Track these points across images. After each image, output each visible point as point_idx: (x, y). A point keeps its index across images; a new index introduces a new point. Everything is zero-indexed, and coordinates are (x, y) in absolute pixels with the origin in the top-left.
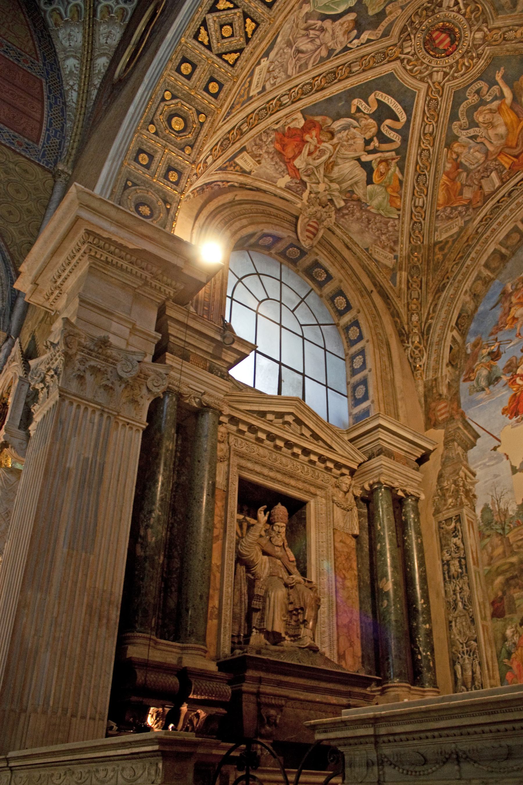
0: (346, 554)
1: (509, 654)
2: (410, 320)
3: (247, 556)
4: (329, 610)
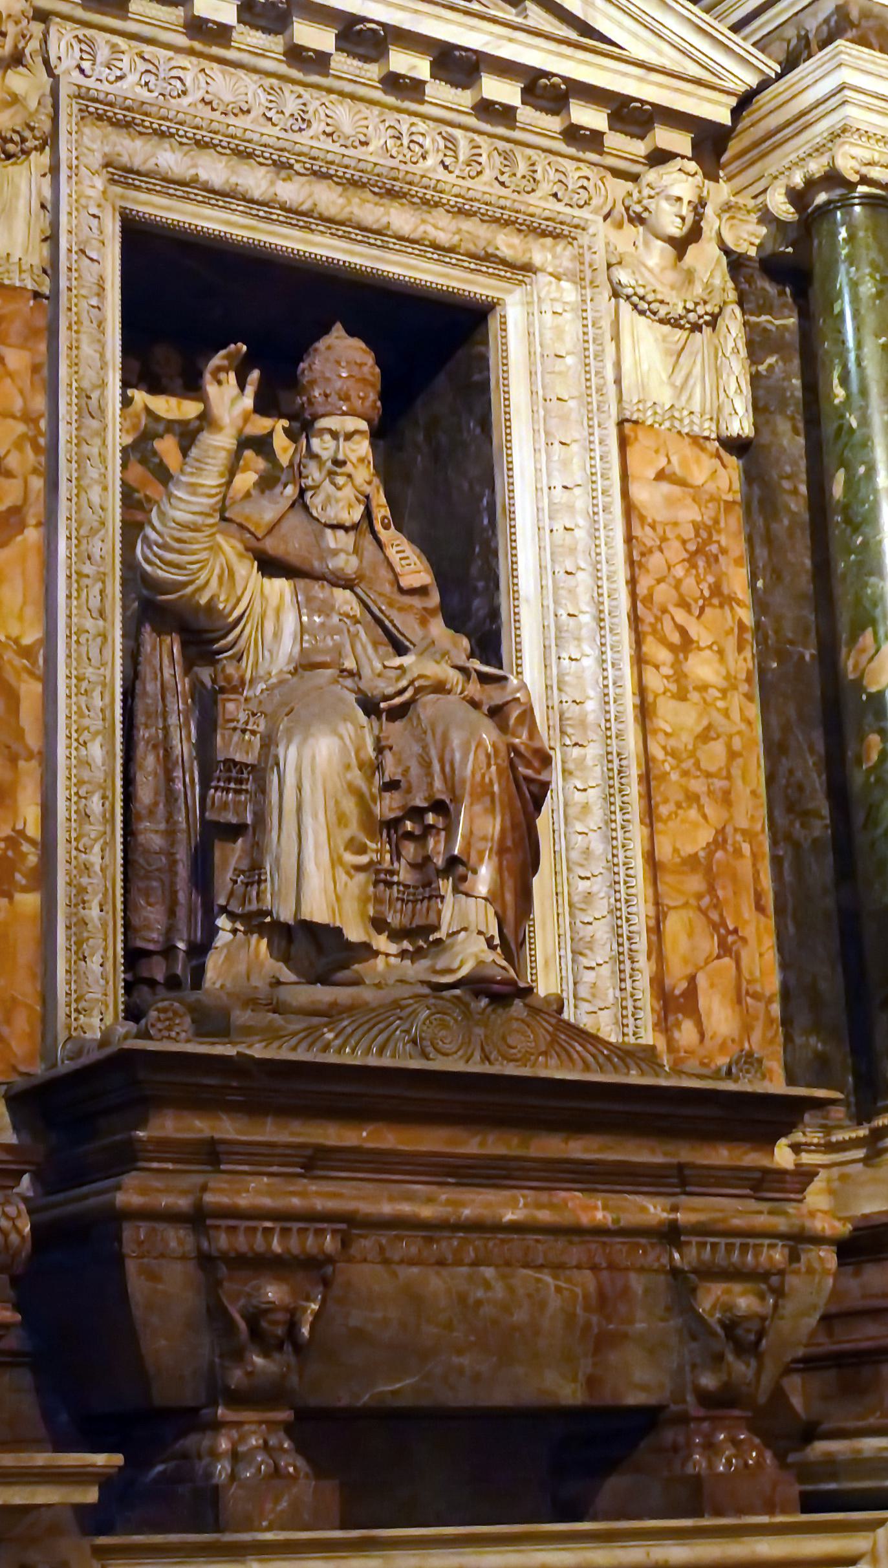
0: (689, 532)
3: (185, 585)
4: (608, 799)
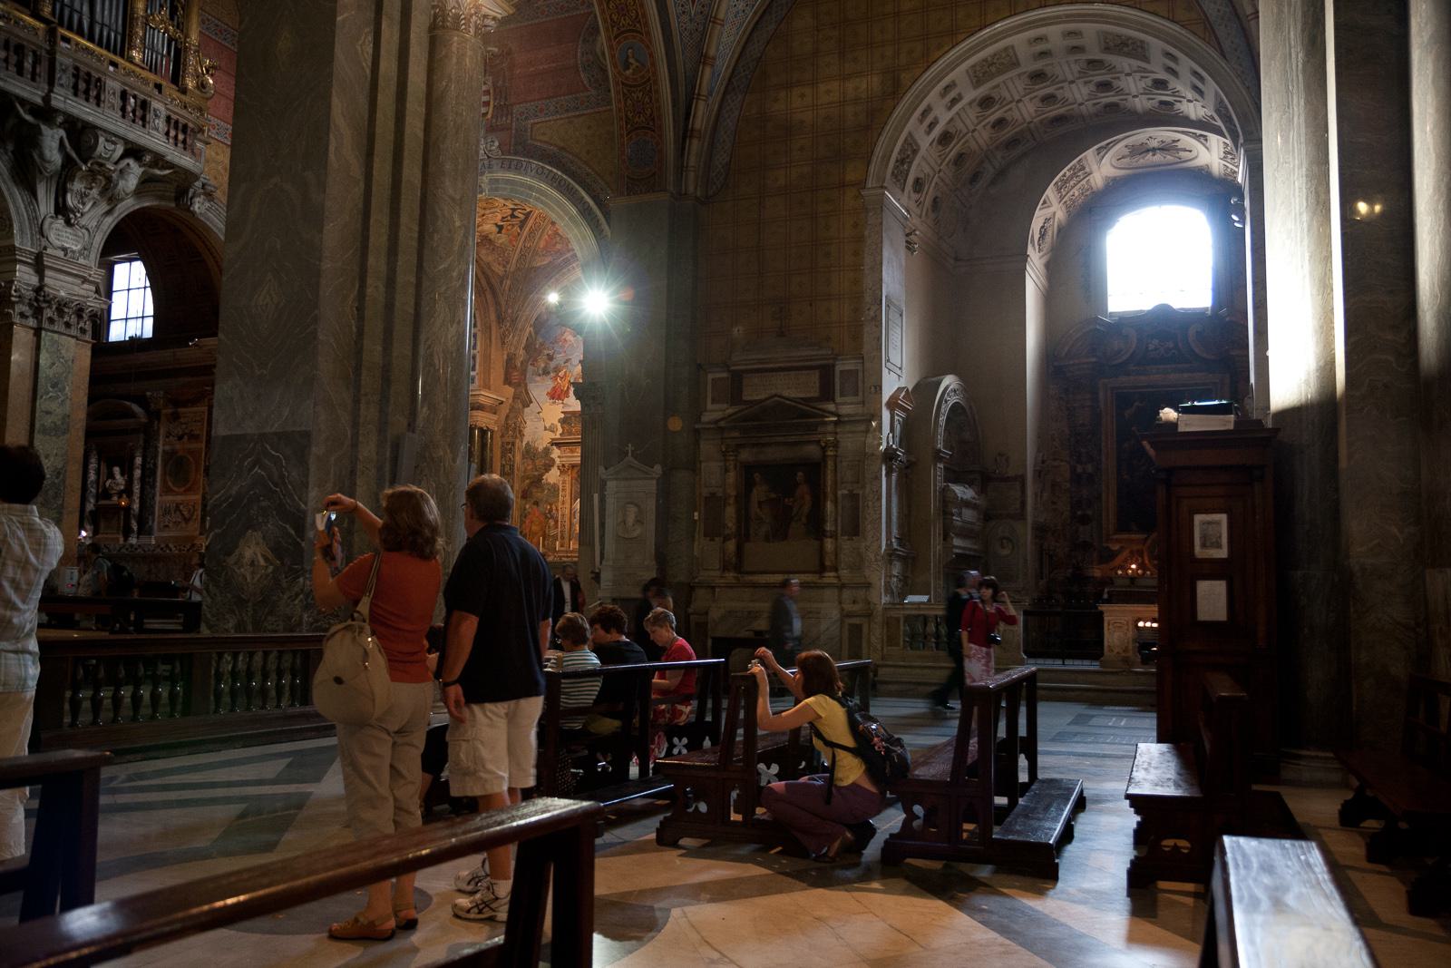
1: (525, 517)
2: (506, 311)
